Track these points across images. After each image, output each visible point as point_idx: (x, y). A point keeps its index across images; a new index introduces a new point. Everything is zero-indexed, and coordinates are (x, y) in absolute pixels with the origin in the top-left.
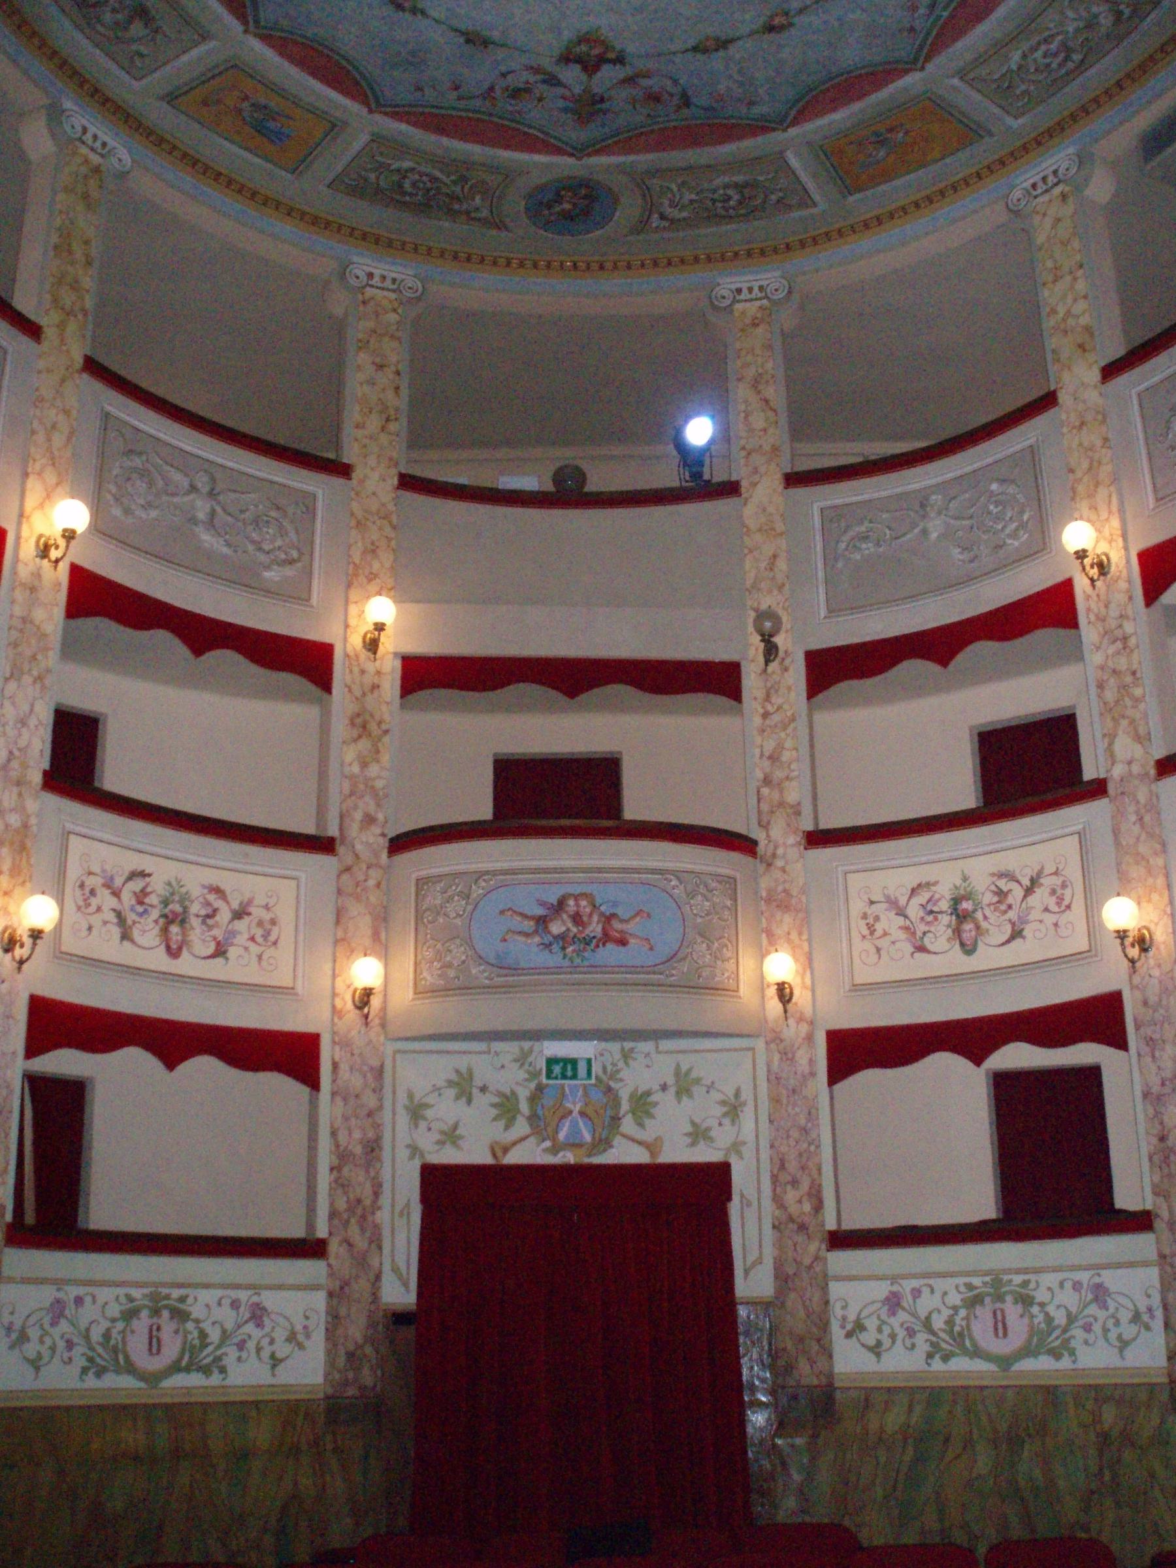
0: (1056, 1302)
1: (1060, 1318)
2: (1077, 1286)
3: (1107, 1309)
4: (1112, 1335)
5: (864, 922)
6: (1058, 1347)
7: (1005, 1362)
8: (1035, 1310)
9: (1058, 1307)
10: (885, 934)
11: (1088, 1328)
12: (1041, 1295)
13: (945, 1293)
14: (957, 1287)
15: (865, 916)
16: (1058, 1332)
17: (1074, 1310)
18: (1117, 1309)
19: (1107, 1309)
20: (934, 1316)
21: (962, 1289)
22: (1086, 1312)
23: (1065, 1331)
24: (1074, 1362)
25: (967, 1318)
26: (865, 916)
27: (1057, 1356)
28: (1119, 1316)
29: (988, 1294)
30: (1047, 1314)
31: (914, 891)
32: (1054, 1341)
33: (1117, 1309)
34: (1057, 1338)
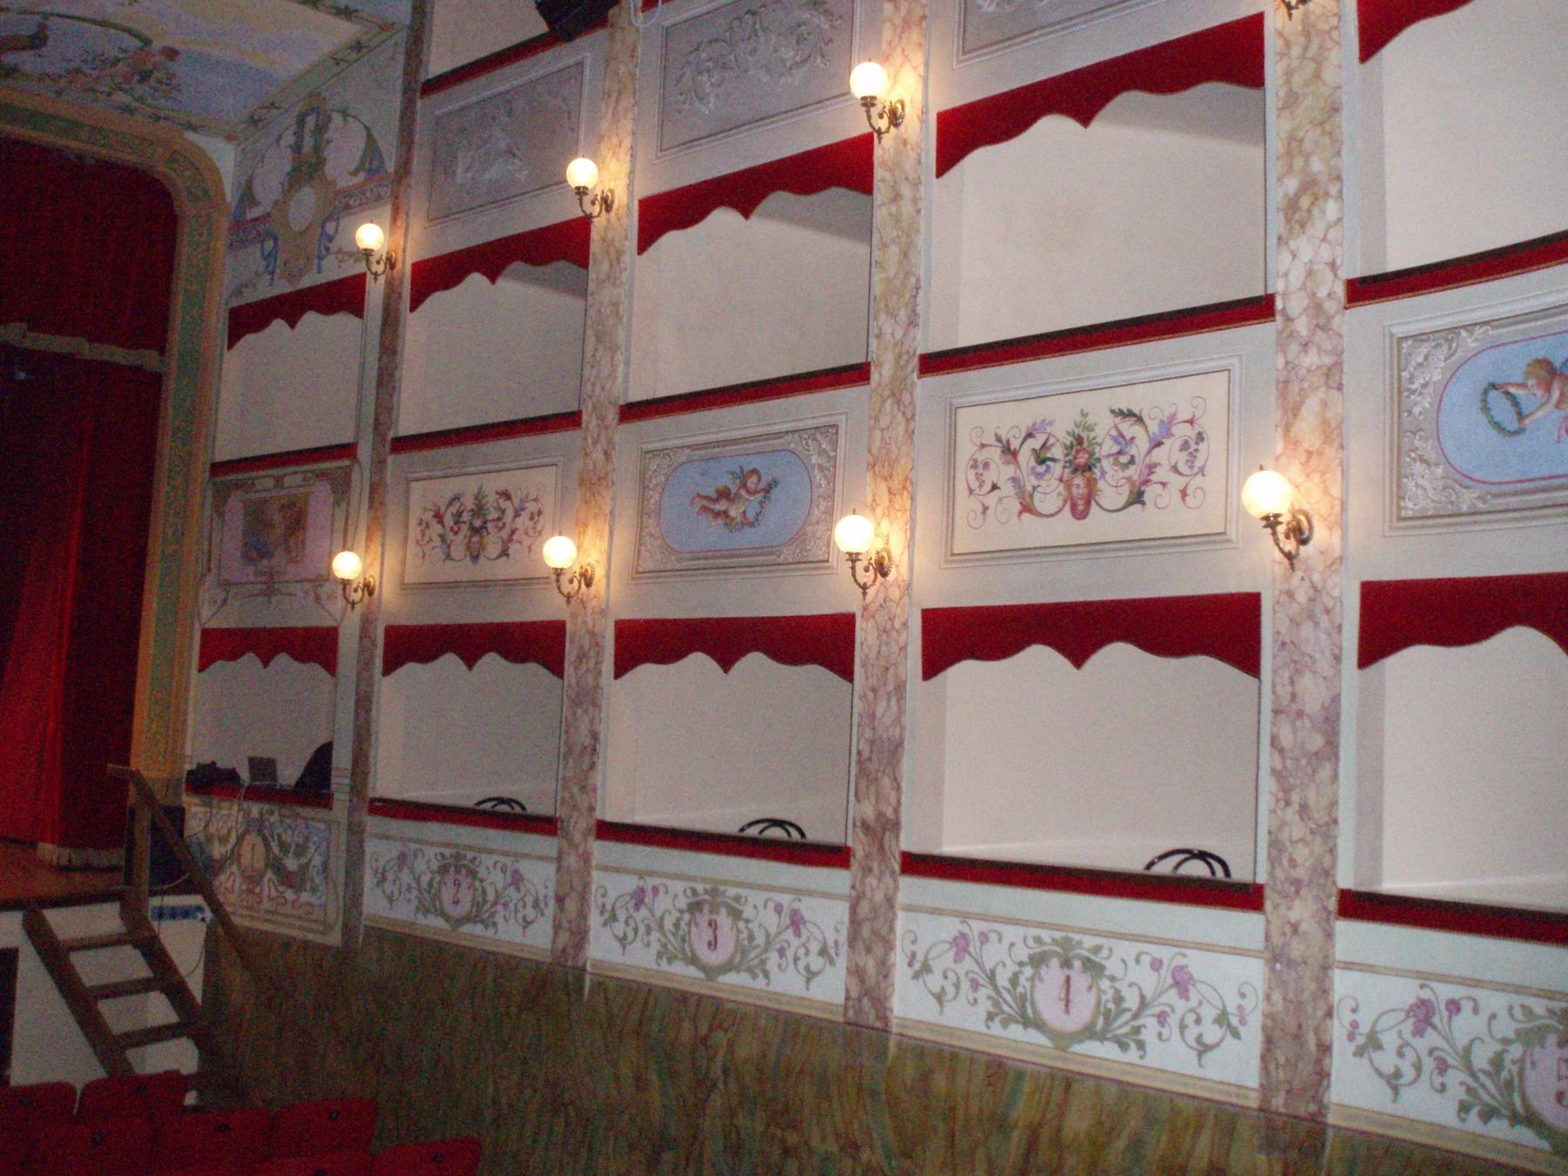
0: (1128, 979)
1: (1132, 1002)
2: (1157, 965)
3: (1187, 999)
4: (1192, 1033)
5: (973, 472)
6: (1126, 1035)
7: (1062, 1039)
8: (1105, 984)
9: (1131, 985)
10: (995, 487)
11: (1162, 1018)
12: (1113, 967)
13: (1012, 945)
14: (1025, 939)
15: (974, 466)
16: (1126, 1016)
17: (1149, 994)
18: (1200, 1003)
19: (1187, 999)
20: (999, 970)
21: (1031, 942)
22: (1164, 999)
23: (1136, 1016)
24: (1142, 1057)
25: (1032, 979)
26: (974, 466)
27: (1124, 1047)
28: (1200, 1011)
29: (1056, 954)
30: (1117, 991)
31: (1030, 435)
32: (1121, 1026)
33: (1200, 1003)
34: (1126, 1023)
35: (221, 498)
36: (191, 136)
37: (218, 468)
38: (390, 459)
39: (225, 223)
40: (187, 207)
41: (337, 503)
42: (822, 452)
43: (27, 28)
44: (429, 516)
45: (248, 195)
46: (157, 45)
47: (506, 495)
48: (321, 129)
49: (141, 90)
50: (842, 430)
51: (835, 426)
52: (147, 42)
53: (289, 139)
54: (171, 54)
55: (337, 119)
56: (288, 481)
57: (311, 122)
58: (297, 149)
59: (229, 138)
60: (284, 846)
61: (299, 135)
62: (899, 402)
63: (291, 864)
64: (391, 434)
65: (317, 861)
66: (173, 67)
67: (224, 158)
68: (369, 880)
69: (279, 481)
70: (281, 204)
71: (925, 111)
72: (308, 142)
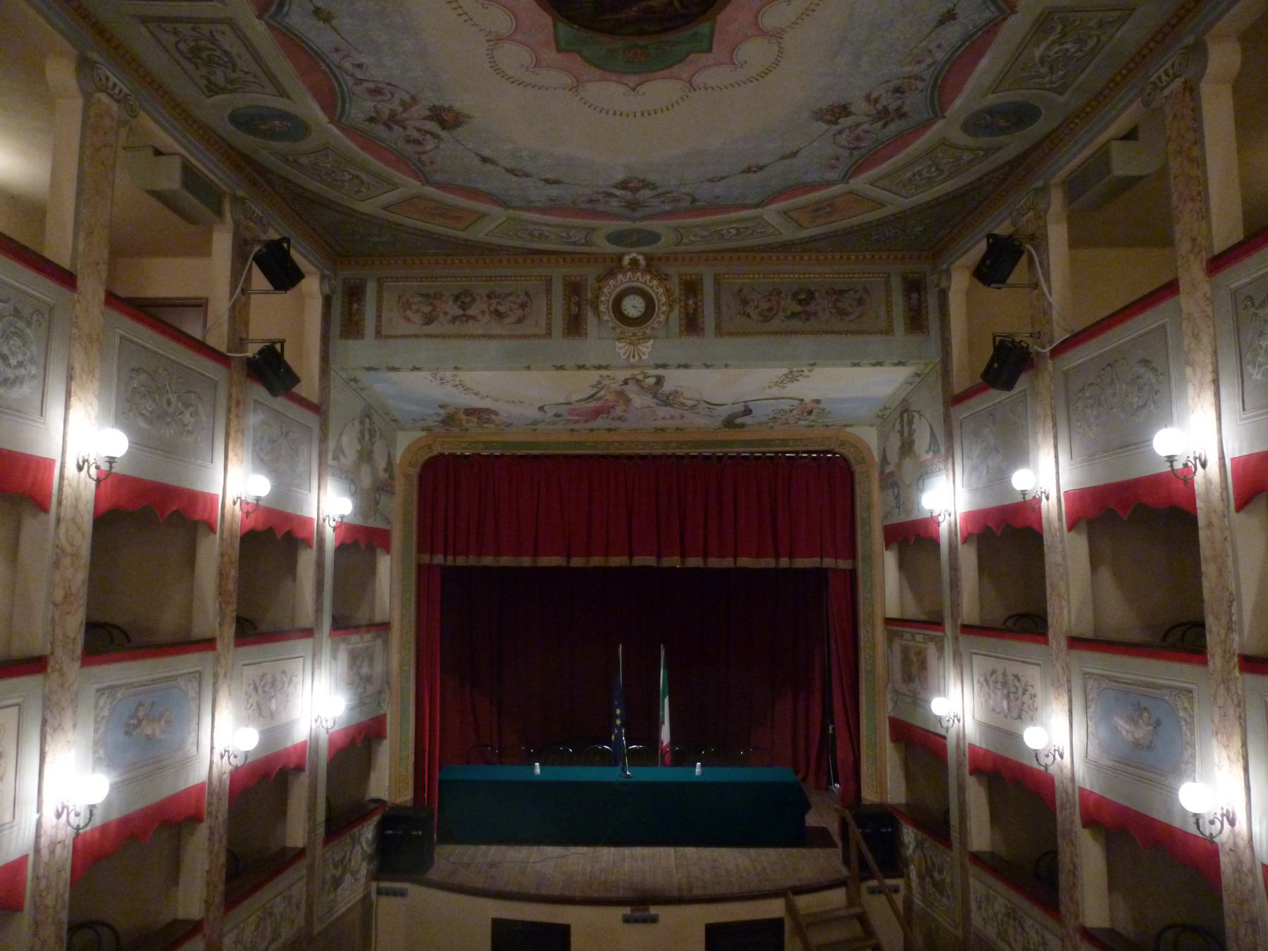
35: (891, 637)
36: (848, 429)
37: (889, 621)
38: (961, 638)
39: (875, 476)
40: (857, 469)
41: (939, 659)
42: (1185, 709)
43: (741, 408)
44: (982, 679)
45: (884, 460)
46: (807, 400)
47: (1017, 677)
48: (910, 423)
49: (812, 417)
50: (1195, 695)
51: (1190, 691)
52: (802, 400)
53: (898, 427)
54: (818, 401)
55: (916, 416)
56: (919, 638)
57: (905, 415)
58: (901, 432)
59: (871, 425)
60: (933, 865)
61: (902, 426)
62: (1228, 689)
63: (937, 877)
64: (960, 622)
65: (948, 880)
66: (821, 406)
67: (870, 438)
68: (974, 906)
69: (913, 635)
70: (899, 465)
71: (1222, 458)
72: (906, 429)
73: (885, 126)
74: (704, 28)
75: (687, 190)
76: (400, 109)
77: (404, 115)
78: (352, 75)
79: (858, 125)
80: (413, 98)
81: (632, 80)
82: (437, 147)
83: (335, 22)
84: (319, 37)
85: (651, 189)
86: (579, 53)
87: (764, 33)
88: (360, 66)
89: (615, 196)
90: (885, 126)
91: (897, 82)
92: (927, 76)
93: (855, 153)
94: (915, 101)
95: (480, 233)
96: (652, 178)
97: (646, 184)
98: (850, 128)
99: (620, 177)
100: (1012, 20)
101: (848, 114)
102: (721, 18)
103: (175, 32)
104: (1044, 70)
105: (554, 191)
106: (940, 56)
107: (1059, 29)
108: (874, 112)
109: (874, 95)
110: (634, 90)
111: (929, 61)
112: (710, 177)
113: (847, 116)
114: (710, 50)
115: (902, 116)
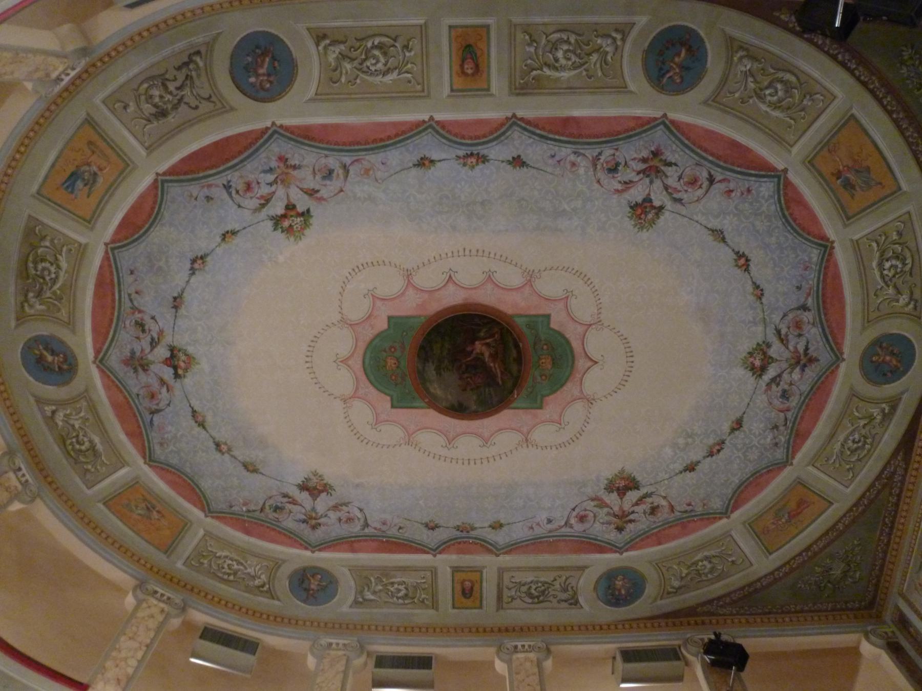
73: (670, 164)
74: (519, 321)
75: (776, 318)
76: (606, 510)
77: (616, 509)
78: (561, 527)
79: (666, 188)
80: (593, 500)
81: (581, 363)
82: (665, 498)
83: (502, 521)
84: (519, 532)
85: (769, 346)
86: (543, 396)
87: (529, 283)
88: (549, 521)
89: (780, 376)
90: (670, 164)
91: (601, 175)
92: (591, 153)
93: (719, 177)
94: (632, 152)
95: (843, 493)
96: (747, 345)
97: (762, 349)
98: (670, 194)
99: (741, 373)
100: (520, 114)
101: (648, 200)
102: (510, 311)
103: (513, 599)
104: (594, 57)
105: (755, 426)
106: (565, 151)
107: (535, 73)
108: (647, 180)
109: (620, 187)
110: (596, 363)
111: (572, 158)
112: (752, 298)
113: (650, 201)
114: (548, 317)
115: (656, 154)
